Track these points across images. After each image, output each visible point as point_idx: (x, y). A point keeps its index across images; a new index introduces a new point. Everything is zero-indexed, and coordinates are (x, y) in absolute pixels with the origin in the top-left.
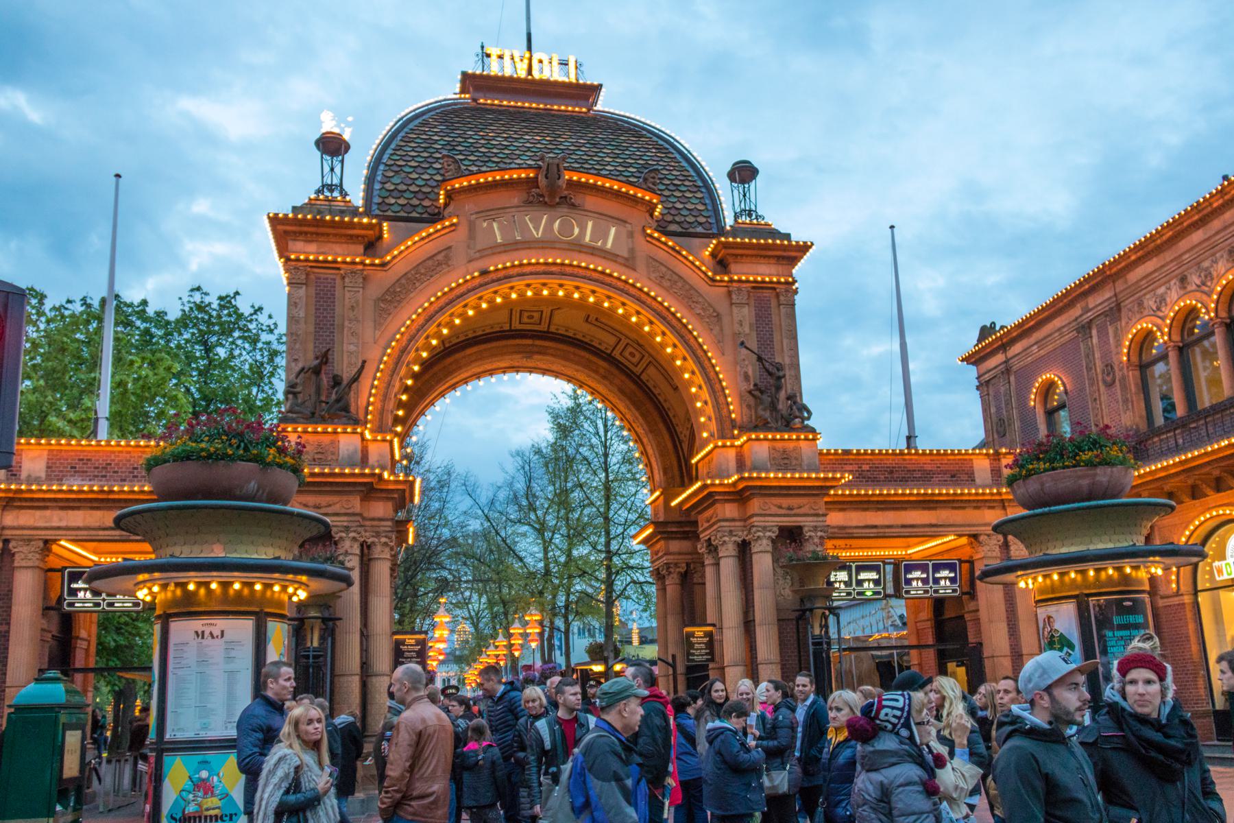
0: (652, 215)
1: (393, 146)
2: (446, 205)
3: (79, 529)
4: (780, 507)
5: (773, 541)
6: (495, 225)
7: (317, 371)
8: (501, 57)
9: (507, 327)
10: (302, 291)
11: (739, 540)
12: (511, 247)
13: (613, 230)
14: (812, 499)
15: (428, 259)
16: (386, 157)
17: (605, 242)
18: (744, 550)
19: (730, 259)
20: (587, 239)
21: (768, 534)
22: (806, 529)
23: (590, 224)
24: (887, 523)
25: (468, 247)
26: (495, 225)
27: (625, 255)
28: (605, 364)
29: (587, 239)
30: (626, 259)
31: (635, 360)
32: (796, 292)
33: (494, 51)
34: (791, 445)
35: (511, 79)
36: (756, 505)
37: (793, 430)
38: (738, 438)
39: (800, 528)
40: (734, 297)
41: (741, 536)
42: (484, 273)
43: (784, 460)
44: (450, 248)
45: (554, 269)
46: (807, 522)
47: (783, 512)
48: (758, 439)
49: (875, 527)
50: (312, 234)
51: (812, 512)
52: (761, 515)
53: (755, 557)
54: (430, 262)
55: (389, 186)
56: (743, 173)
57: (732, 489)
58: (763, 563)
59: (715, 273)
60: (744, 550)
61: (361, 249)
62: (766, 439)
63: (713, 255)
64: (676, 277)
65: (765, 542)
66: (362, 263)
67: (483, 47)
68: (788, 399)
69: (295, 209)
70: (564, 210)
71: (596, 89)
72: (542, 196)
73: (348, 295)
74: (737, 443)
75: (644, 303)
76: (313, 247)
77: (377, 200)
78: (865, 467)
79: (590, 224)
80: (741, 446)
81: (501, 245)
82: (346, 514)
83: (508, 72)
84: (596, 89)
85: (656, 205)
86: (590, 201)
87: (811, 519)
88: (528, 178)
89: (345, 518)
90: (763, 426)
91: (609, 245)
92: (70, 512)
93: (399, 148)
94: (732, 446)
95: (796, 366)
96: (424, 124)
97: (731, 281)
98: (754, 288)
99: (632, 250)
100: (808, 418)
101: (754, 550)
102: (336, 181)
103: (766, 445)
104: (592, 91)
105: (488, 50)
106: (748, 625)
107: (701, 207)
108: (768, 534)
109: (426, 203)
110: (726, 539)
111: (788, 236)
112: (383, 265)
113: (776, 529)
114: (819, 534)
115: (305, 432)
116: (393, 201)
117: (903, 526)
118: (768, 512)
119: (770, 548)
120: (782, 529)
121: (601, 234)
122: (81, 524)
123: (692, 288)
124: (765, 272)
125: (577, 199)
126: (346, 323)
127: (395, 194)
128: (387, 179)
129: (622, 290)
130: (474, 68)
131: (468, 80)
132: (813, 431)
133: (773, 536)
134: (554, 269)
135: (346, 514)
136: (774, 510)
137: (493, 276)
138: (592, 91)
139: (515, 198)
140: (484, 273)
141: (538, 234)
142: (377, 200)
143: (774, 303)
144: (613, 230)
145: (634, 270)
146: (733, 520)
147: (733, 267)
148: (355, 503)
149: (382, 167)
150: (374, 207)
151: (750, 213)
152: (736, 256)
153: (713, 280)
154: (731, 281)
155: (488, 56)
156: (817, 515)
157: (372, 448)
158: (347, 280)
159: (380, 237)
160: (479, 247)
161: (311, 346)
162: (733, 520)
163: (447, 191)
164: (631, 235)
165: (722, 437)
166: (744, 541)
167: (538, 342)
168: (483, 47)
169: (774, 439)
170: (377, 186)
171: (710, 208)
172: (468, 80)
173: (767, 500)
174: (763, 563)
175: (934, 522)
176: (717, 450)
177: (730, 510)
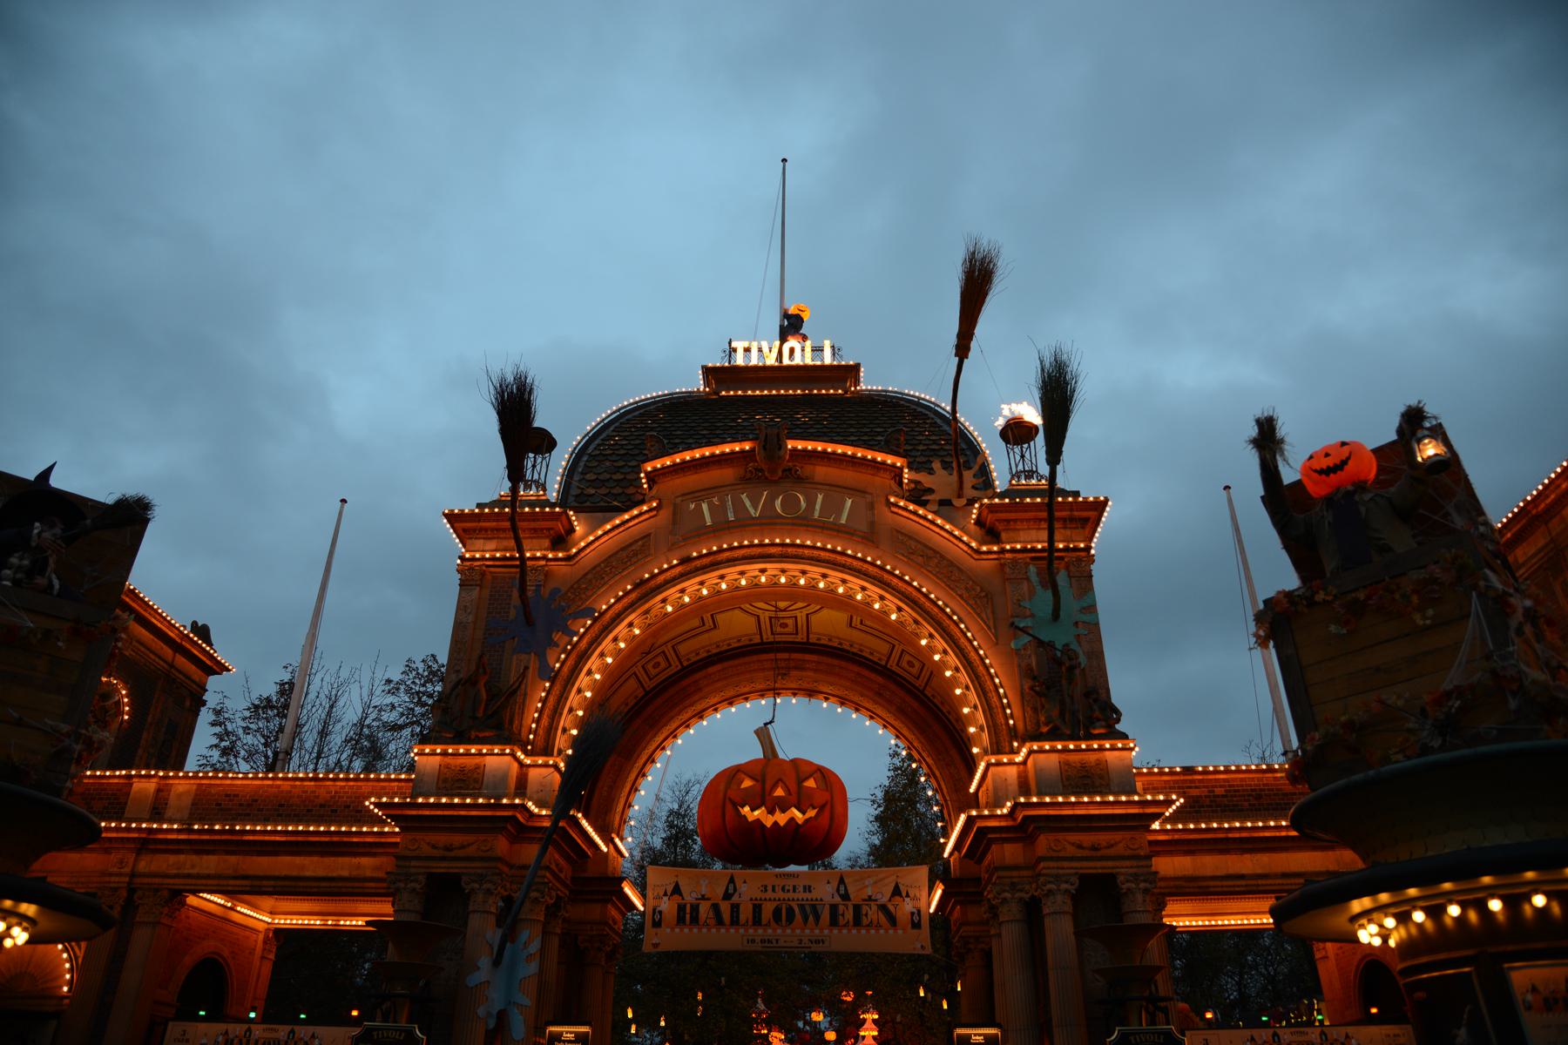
0: (900, 483)
2: (650, 488)
5: (1074, 898)
6: (705, 506)
7: (472, 681)
8: (747, 350)
9: (757, 640)
10: (475, 593)
11: (1026, 896)
12: (722, 528)
13: (849, 502)
15: (623, 549)
18: (1033, 913)
19: (1000, 527)
20: (817, 514)
21: (1064, 886)
22: (1122, 878)
23: (820, 497)
26: (705, 506)
28: (880, 680)
29: (817, 514)
31: (915, 671)
33: (739, 345)
34: (1092, 757)
35: (765, 368)
36: (1044, 843)
37: (1090, 737)
38: (1017, 752)
39: (1113, 877)
42: (686, 560)
43: (1088, 779)
45: (773, 550)
46: (1124, 869)
47: (1086, 853)
48: (1041, 751)
50: (493, 529)
51: (1129, 852)
52: (1051, 859)
53: (1048, 921)
54: (624, 554)
55: (588, 477)
57: (1010, 823)
58: (1060, 930)
59: (982, 543)
61: (546, 543)
62: (1053, 750)
63: (978, 522)
64: (930, 553)
65: (1059, 898)
66: (544, 558)
68: (1087, 695)
69: (479, 505)
71: (855, 368)
72: (761, 470)
74: (1019, 759)
75: (888, 585)
76: (492, 545)
77: (574, 491)
78: (1219, 791)
79: (820, 497)
80: (1024, 762)
82: (482, 859)
83: (754, 361)
84: (855, 368)
85: (901, 469)
86: (821, 472)
87: (1128, 863)
88: (742, 452)
90: (1054, 735)
91: (843, 521)
93: (610, 437)
94: (1011, 763)
95: (1097, 655)
96: (641, 415)
97: (1003, 551)
98: (1033, 559)
99: (872, 524)
100: (1118, 721)
101: (1046, 911)
102: (536, 477)
103: (1054, 757)
104: (850, 372)
105: (734, 345)
108: (1064, 886)
109: (631, 490)
110: (1007, 895)
111: (1076, 494)
112: (568, 558)
114: (1142, 885)
115: (444, 754)
118: (1062, 854)
119: (1068, 908)
120: (1083, 878)
121: (833, 507)
123: (951, 564)
125: (808, 470)
128: (587, 470)
129: (859, 571)
130: (717, 361)
131: (708, 372)
132: (1124, 736)
133: (1072, 889)
134: (773, 550)
135: (482, 859)
136: (1071, 851)
137: (698, 563)
138: (850, 372)
139: (727, 474)
140: (686, 560)
142: (574, 491)
144: (849, 502)
147: (1004, 536)
148: (501, 845)
150: (571, 499)
151: (1030, 474)
152: (1008, 521)
153: (978, 552)
154: (1003, 551)
155: (735, 350)
156: (1137, 857)
157: (534, 774)
159: (572, 530)
162: (1016, 867)
163: (647, 474)
165: (997, 751)
167: (794, 656)
169: (1065, 750)
170: (576, 477)
172: (708, 372)
173: (1061, 836)
174: (1060, 930)
176: (992, 769)
177: (1010, 853)
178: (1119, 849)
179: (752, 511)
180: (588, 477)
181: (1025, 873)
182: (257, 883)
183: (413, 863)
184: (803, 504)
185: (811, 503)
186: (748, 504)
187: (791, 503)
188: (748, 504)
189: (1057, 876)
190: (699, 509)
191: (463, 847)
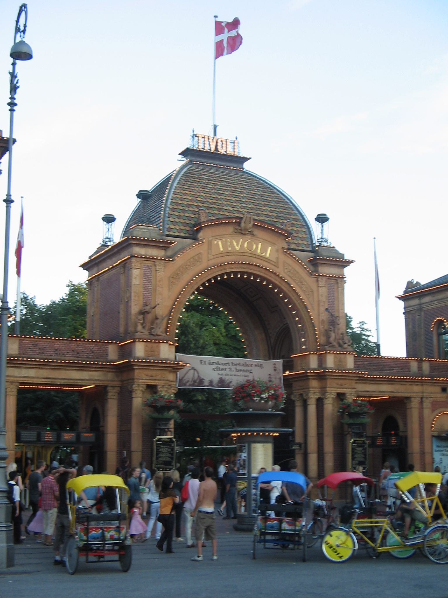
1: (170, 197)
3: (33, 378)
4: (338, 384)
13: (270, 248)
14: (350, 381)
16: (169, 203)
17: (266, 254)
18: (320, 402)
23: (260, 244)
24: (373, 390)
25: (208, 253)
27: (274, 260)
30: (275, 263)
32: (345, 282)
40: (320, 283)
41: (317, 396)
44: (200, 253)
49: (368, 391)
51: (350, 387)
56: (322, 219)
60: (320, 402)
67: (193, 131)
70: (248, 236)
73: (158, 274)
81: (222, 253)
82: (163, 380)
89: (162, 382)
91: (268, 255)
92: (30, 370)
99: (277, 258)
106: (320, 436)
107: (305, 236)
113: (335, 394)
116: (173, 227)
117: (380, 392)
121: (264, 249)
122: (33, 375)
124: (332, 271)
126: (157, 288)
127: (174, 223)
141: (237, 248)
143: (336, 287)
145: (278, 267)
146: (315, 388)
149: (168, 209)
158: (157, 267)
160: (213, 254)
161: (141, 298)
162: (315, 388)
164: (277, 251)
166: (319, 398)
168: (193, 131)
171: (308, 236)
175: (393, 390)
178: (346, 386)
179: (237, 247)
180: (171, 219)
181: (318, 390)
182: (53, 380)
183: (141, 381)
184: (254, 247)
185: (257, 247)
186: (235, 244)
187: (250, 246)
188: (235, 244)
189: (331, 393)
190: (218, 243)
191: (156, 376)
